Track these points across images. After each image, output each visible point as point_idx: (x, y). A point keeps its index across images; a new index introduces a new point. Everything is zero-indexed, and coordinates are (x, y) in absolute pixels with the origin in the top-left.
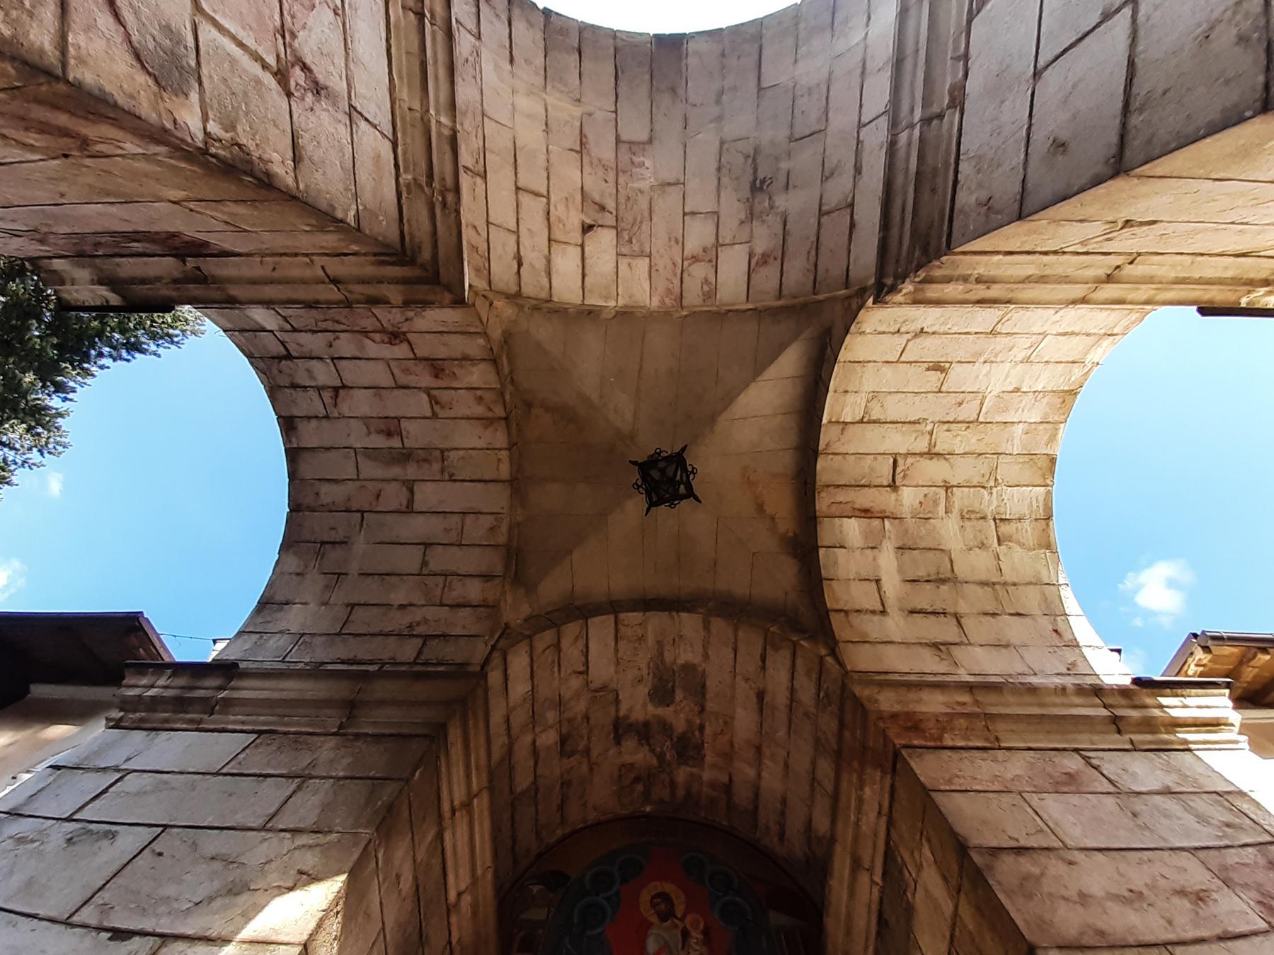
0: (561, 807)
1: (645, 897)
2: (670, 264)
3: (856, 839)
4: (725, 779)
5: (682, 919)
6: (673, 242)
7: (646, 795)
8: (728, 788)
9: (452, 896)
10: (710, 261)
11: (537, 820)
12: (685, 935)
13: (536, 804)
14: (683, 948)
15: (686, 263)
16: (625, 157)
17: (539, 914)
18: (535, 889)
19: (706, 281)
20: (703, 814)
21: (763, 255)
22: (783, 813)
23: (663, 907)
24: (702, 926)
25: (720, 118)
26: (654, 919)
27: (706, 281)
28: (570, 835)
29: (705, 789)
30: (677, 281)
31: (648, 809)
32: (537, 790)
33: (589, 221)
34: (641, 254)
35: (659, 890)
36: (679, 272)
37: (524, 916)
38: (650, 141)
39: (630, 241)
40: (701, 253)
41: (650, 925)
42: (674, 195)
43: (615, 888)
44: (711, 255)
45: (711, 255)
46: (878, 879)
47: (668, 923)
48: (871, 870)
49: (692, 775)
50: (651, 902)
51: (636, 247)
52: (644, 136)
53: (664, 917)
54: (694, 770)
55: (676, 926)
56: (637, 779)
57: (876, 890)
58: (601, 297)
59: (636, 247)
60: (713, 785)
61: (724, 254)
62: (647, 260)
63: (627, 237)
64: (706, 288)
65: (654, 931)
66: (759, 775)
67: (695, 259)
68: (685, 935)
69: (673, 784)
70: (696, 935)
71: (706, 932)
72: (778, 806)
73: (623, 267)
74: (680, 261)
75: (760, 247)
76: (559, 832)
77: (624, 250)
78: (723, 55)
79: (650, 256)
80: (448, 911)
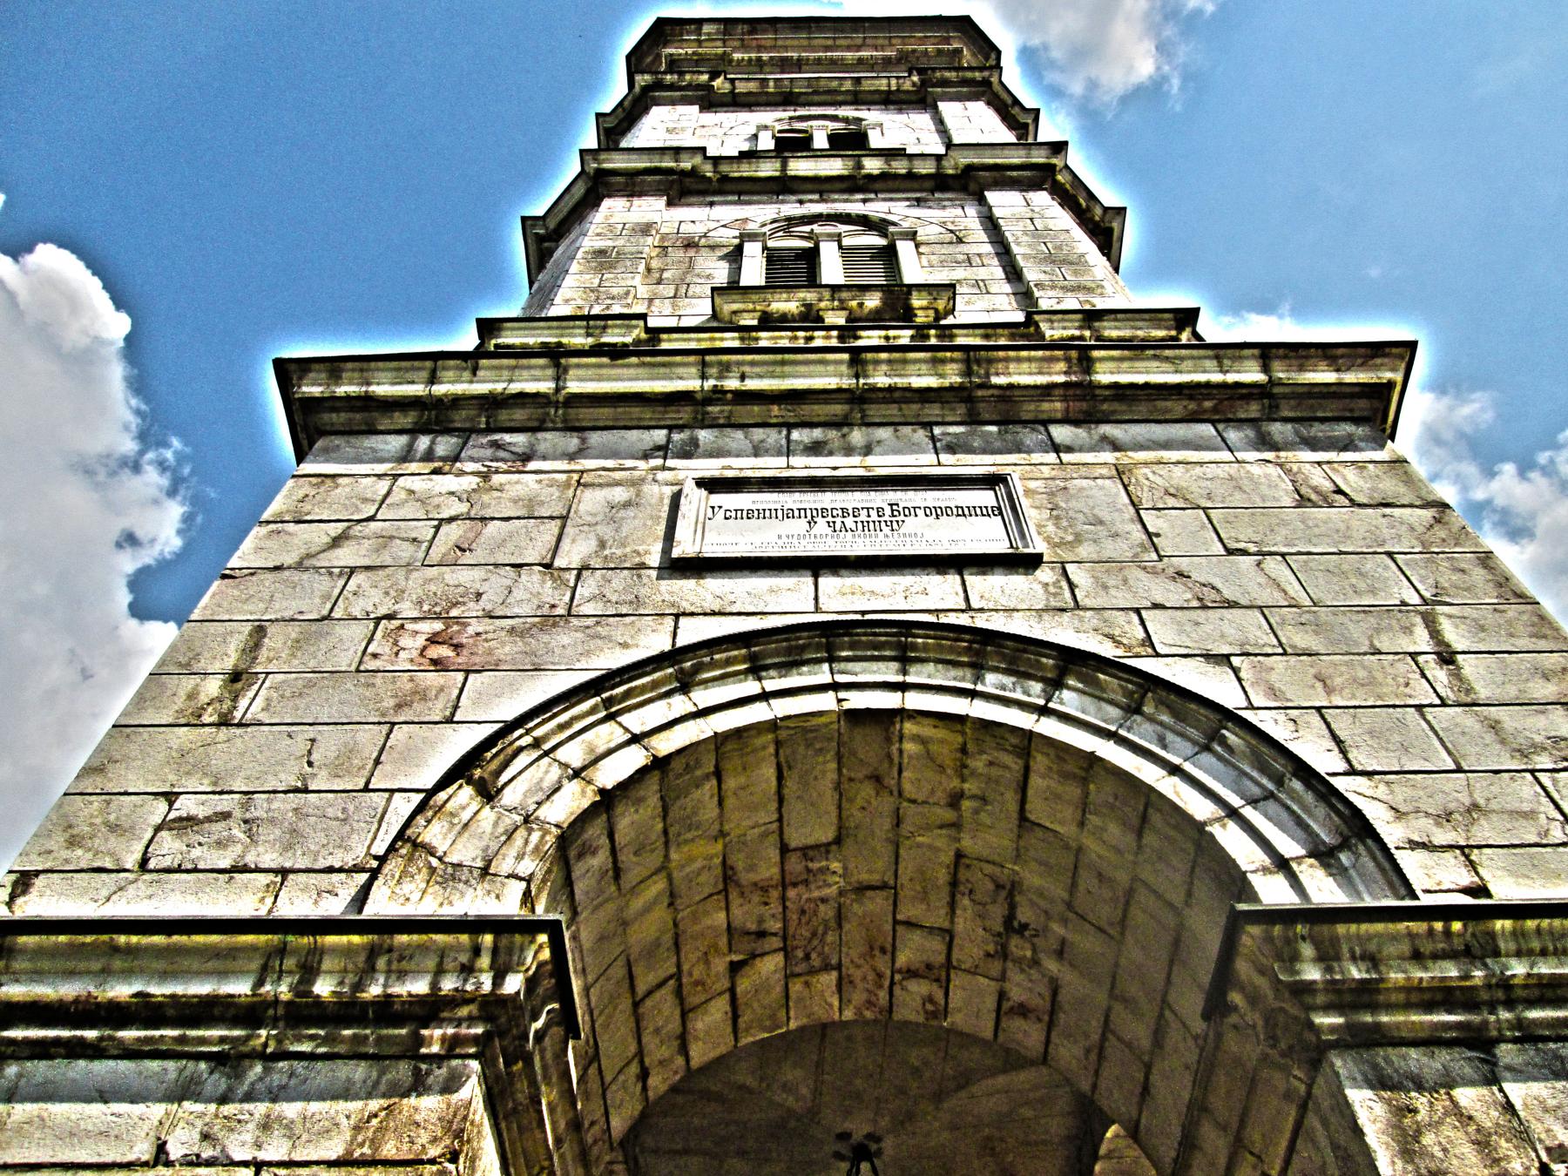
2: (871, 976)
6: (877, 952)
10: (937, 980)
15: (897, 977)
16: (795, 864)
19: (930, 999)
21: (1021, 1005)
25: (956, 825)
27: (930, 999)
30: (883, 995)
33: (735, 958)
34: (826, 967)
36: (887, 983)
38: (838, 841)
39: (807, 957)
40: (923, 966)
42: (877, 904)
44: (941, 973)
45: (941, 973)
51: (816, 961)
52: (827, 835)
58: (765, 1029)
59: (816, 961)
61: (957, 980)
62: (834, 974)
63: (800, 953)
64: (929, 1007)
67: (911, 973)
73: (796, 987)
74: (888, 973)
75: (1016, 995)
77: (797, 970)
78: (963, 750)
79: (839, 967)
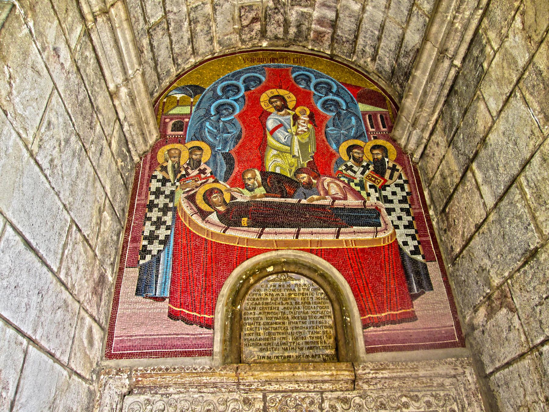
0: (191, 40)
1: (264, 98)
3: (448, 35)
4: (331, 15)
5: (294, 109)
7: (263, 33)
8: (334, 25)
9: (112, 87)
11: (172, 49)
12: (296, 118)
13: (170, 36)
14: (294, 125)
17: (186, 110)
18: (179, 96)
20: (310, 47)
22: (379, 39)
23: (279, 103)
24: (308, 112)
26: (272, 110)
28: (201, 63)
29: (313, 26)
31: (265, 44)
32: (168, 24)
35: (276, 94)
37: (171, 112)
41: (270, 113)
43: (241, 94)
46: (457, 62)
47: (283, 112)
48: (452, 59)
49: (303, 14)
50: (269, 101)
53: (279, 109)
54: (305, 10)
55: (289, 114)
56: (255, 20)
57: (453, 72)
60: (321, 21)
65: (271, 116)
66: (363, 9)
68: (296, 118)
69: (286, 24)
70: (304, 118)
71: (311, 116)
72: (377, 33)
76: (192, 60)
80: (111, 96)
